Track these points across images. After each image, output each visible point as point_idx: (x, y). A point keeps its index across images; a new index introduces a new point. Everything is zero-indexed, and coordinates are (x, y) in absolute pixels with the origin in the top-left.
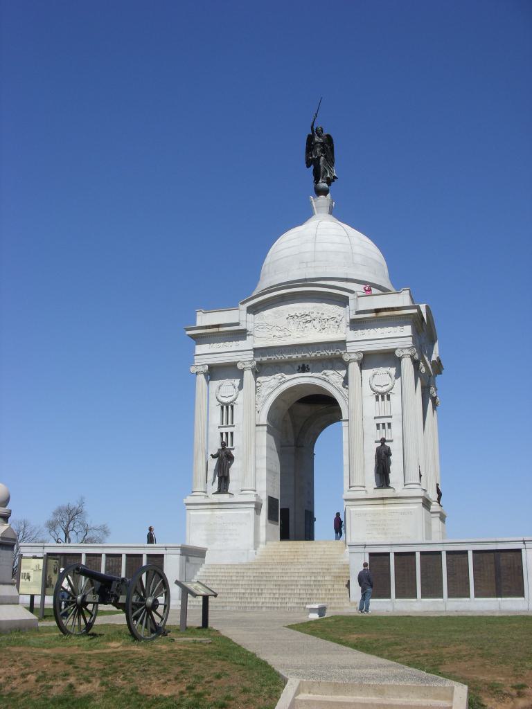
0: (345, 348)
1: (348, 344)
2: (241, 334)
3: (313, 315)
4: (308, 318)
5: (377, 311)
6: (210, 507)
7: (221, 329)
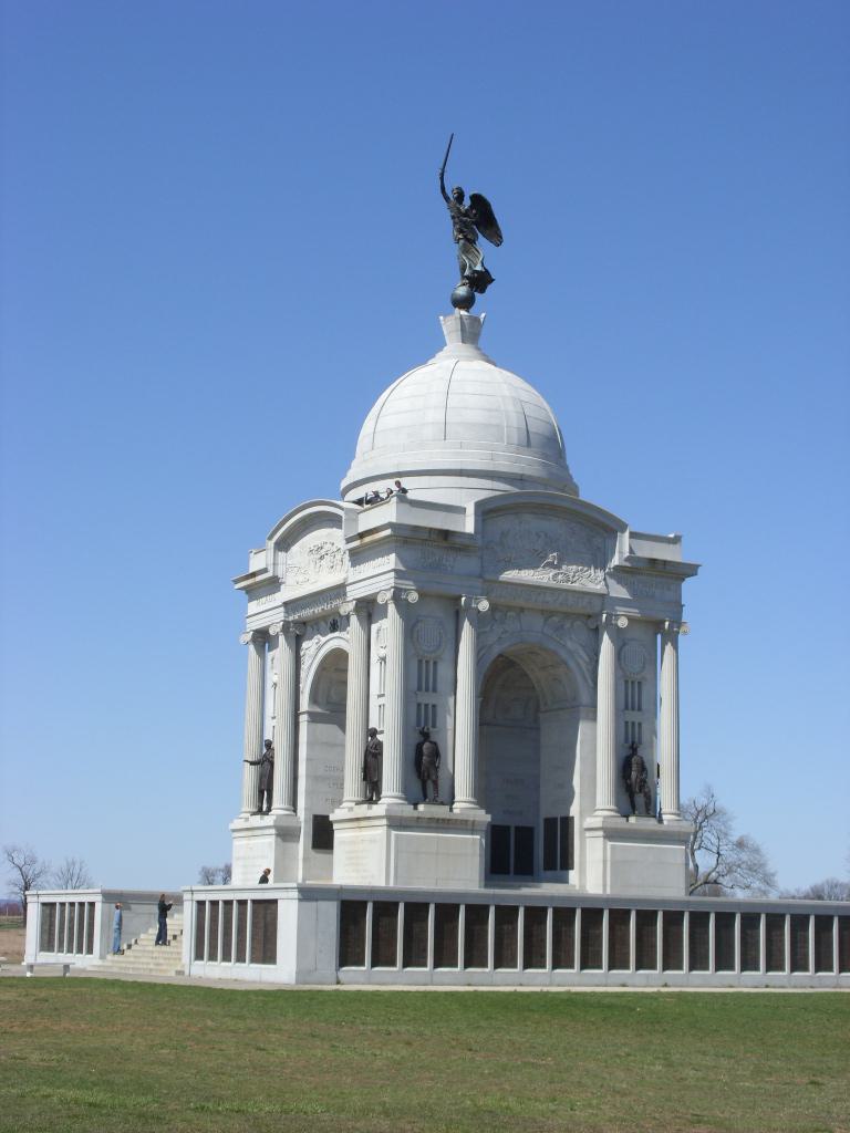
0: (345, 594)
1: (348, 589)
2: (274, 584)
3: (327, 547)
4: (323, 552)
5: (361, 536)
6: (250, 833)
7: (259, 578)
